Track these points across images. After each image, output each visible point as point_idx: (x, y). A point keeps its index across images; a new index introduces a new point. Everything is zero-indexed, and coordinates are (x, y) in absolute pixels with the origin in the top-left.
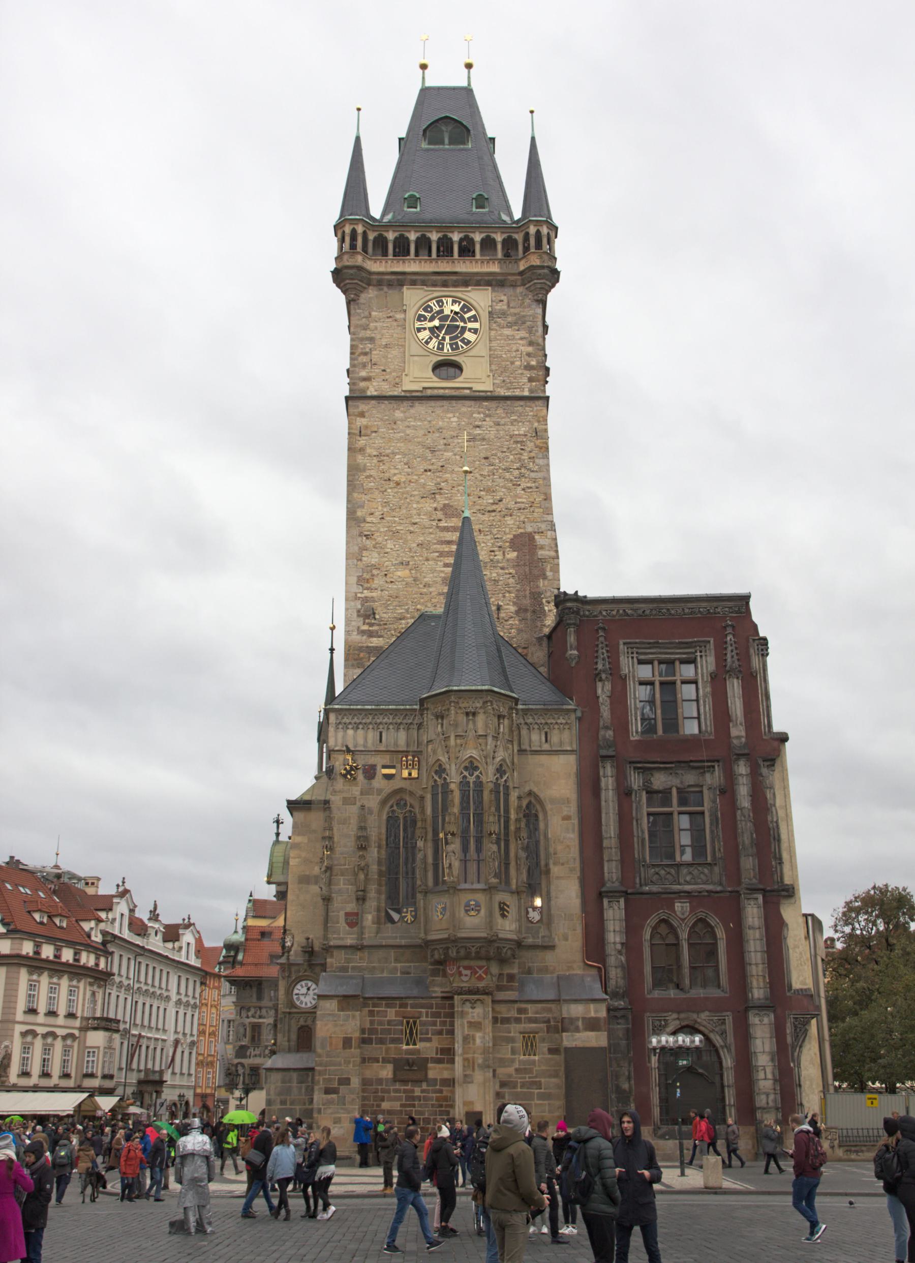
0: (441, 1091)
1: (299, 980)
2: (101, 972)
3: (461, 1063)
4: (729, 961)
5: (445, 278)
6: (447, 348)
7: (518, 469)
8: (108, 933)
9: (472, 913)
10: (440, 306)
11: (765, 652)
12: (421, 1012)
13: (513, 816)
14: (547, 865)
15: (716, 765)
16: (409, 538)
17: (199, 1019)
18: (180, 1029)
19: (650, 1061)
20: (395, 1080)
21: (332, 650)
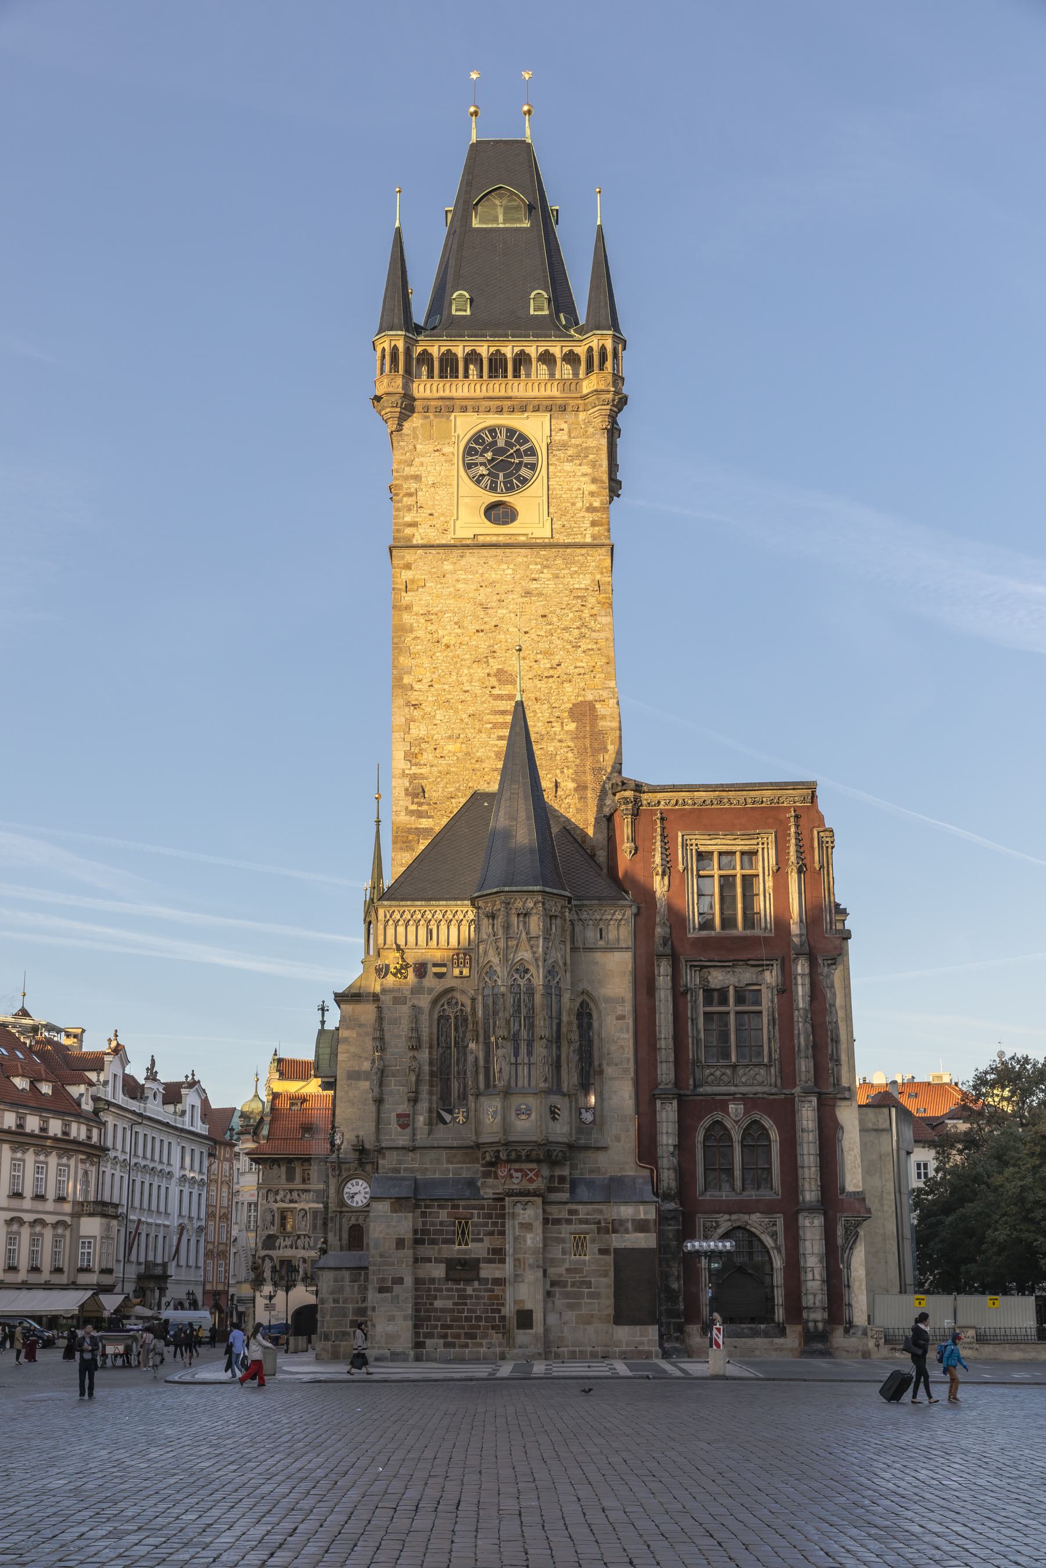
0: (492, 1291)
1: (349, 1178)
2: (93, 1146)
3: (512, 1264)
4: (782, 1163)
5: (499, 403)
6: (501, 486)
7: (578, 628)
8: (99, 1099)
9: (523, 1117)
10: (493, 437)
11: (830, 845)
12: (472, 1214)
13: (565, 1018)
14: (600, 1065)
15: (775, 963)
16: (460, 707)
17: (207, 1199)
18: (185, 1212)
19: (700, 1262)
20: (448, 1279)
21: (378, 822)
